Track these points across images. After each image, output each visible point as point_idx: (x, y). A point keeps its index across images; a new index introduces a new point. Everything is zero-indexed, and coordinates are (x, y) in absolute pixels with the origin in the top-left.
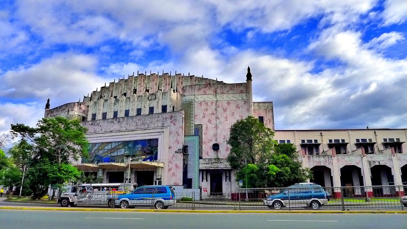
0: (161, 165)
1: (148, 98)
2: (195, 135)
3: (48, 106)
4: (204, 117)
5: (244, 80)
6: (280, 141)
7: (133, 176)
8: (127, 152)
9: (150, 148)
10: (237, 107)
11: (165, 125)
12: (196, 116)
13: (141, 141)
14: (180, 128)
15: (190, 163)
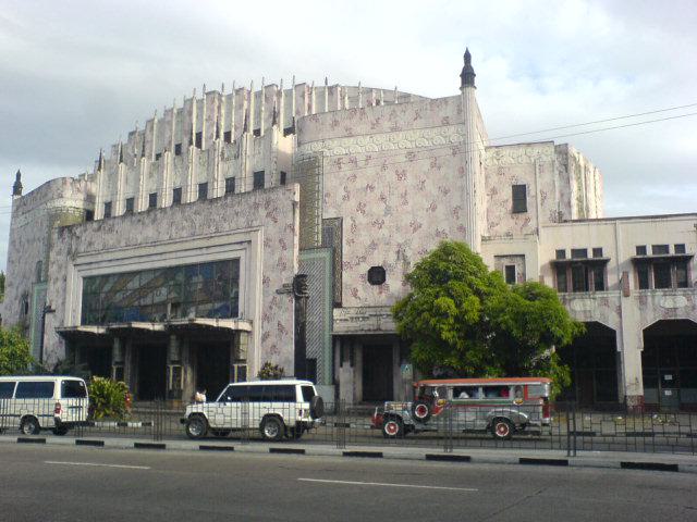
0: (244, 326)
1: (223, 154)
2: (324, 246)
3: (17, 188)
4: (346, 198)
5: (453, 87)
6: (573, 251)
7: (185, 354)
8: (173, 295)
9: (220, 282)
10: (433, 165)
11: (255, 223)
12: (328, 195)
13: (202, 265)
14: (288, 231)
15: (312, 318)
